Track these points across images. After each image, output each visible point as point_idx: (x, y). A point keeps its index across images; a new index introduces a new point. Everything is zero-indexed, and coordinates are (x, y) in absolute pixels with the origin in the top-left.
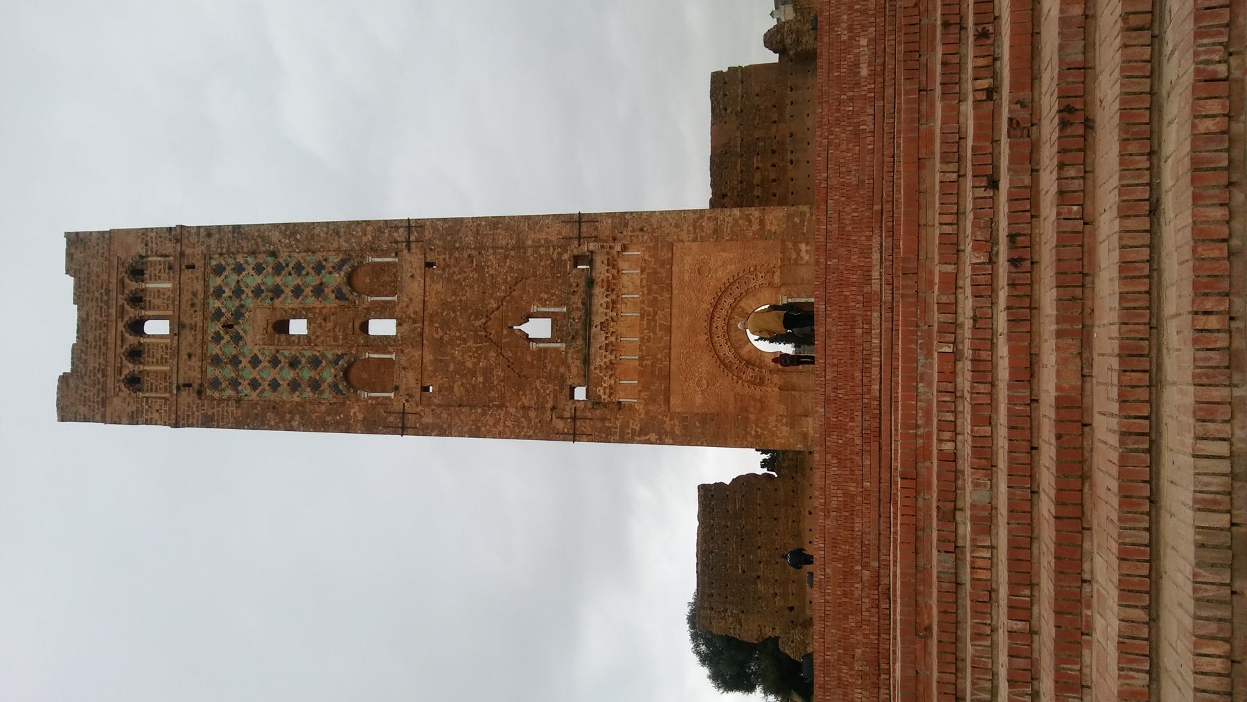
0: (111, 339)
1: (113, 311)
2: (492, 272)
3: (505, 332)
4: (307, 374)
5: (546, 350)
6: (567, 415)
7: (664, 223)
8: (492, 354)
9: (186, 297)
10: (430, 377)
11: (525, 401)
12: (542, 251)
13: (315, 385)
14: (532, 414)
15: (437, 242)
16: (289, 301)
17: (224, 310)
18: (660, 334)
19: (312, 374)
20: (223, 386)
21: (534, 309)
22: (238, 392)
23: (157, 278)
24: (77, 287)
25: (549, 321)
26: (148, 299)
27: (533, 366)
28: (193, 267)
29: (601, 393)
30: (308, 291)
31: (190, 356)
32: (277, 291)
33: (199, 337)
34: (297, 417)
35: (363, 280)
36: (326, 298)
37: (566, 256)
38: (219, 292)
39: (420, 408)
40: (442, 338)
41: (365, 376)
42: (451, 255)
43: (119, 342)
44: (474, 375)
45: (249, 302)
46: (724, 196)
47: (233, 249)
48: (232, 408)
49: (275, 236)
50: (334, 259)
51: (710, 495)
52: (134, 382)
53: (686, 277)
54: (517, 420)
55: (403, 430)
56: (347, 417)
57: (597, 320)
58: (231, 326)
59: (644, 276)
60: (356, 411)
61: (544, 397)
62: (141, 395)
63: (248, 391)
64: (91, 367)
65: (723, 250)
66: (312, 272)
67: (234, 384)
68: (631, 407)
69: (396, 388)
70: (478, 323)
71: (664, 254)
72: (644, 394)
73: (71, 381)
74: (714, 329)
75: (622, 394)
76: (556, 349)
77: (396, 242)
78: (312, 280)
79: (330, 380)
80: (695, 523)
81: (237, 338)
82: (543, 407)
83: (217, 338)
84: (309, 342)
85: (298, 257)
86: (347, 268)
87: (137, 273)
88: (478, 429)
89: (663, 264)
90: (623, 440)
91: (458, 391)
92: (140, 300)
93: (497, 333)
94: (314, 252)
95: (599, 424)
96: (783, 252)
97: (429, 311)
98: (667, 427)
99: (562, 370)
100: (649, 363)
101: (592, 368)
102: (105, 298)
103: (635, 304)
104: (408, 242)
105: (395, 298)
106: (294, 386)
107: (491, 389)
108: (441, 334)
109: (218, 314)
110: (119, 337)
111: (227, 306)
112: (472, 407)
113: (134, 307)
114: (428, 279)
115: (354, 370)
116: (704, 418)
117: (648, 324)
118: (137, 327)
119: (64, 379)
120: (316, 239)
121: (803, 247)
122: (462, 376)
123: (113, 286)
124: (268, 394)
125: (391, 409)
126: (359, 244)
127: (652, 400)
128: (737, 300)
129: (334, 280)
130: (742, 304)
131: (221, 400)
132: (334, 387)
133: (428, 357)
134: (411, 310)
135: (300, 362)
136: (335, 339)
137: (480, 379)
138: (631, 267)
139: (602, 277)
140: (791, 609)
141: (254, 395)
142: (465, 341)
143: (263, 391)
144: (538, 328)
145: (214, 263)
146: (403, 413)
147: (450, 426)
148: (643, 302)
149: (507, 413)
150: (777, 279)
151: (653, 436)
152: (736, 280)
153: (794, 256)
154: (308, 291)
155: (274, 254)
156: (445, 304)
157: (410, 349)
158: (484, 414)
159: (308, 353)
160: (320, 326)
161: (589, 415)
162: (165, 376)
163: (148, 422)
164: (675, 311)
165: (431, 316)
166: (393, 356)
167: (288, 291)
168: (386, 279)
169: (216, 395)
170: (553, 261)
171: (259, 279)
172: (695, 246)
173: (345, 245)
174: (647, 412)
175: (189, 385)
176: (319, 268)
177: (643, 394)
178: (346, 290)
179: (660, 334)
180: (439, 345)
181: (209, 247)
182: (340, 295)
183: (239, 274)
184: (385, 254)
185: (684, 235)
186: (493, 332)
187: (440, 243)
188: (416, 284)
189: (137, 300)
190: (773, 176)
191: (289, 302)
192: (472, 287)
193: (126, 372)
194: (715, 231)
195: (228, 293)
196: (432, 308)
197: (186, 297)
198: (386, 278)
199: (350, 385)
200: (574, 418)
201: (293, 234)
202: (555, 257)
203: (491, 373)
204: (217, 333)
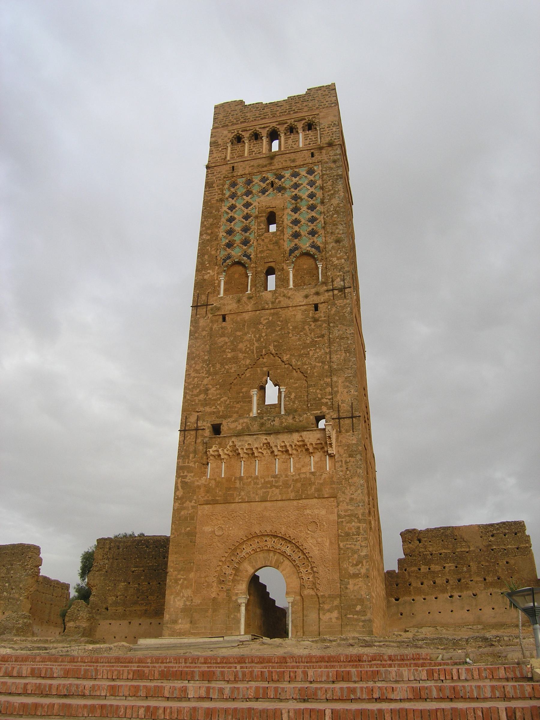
2: (311, 353)
3: (265, 369)
4: (237, 238)
5: (250, 402)
6: (200, 424)
7: (353, 488)
8: (248, 362)
10: (232, 320)
11: (212, 391)
12: (329, 389)
13: (230, 245)
14: (202, 397)
15: (334, 309)
16: (289, 218)
17: (283, 180)
18: (261, 492)
21: (283, 389)
24: (299, 97)
25: (276, 402)
28: (313, 155)
29: (214, 448)
30: (296, 228)
32: (296, 210)
34: (209, 237)
35: (306, 263)
36: (291, 241)
37: (324, 409)
39: (210, 316)
40: (261, 323)
41: (236, 276)
42: (324, 321)
43: (263, 126)
44: (233, 350)
45: (288, 195)
46: (420, 541)
47: (325, 177)
48: (217, 197)
52: (239, 139)
53: (308, 512)
55: (196, 306)
56: (207, 268)
57: (271, 439)
58: (272, 186)
59: (308, 475)
61: (214, 405)
62: (229, 145)
65: (331, 543)
66: (310, 228)
67: (233, 196)
68: (204, 473)
70: (271, 348)
71: (327, 491)
73: (240, 107)
74: (265, 539)
75: (214, 465)
76: (251, 410)
77: (332, 281)
79: (233, 253)
81: (264, 191)
82: (207, 405)
84: (259, 236)
85: (321, 218)
87: (310, 126)
88: (193, 359)
89: (318, 490)
90: (179, 468)
91: (221, 341)
92: (291, 132)
93: (264, 363)
95: (192, 449)
96: (330, 597)
97: (281, 312)
98: (188, 504)
99: (235, 415)
100: (238, 485)
101: (233, 439)
104: (333, 290)
107: (222, 364)
109: (280, 177)
110: (265, 125)
112: (209, 352)
113: (286, 129)
114: (305, 307)
115: (241, 268)
116: (192, 534)
117: (268, 482)
119: (242, 102)
121: (335, 614)
122: (232, 342)
124: (226, 217)
125: (210, 295)
128: (288, 557)
129: (305, 244)
130: (287, 562)
132: (229, 257)
133: (246, 316)
134: (281, 299)
135: (246, 232)
137: (229, 356)
138: (316, 463)
139: (306, 440)
140: (107, 609)
141: (225, 209)
142: (258, 340)
143: (227, 213)
144: (272, 394)
145: (315, 168)
146: (207, 305)
147: (196, 338)
148: (287, 476)
149: (204, 378)
150: (306, 592)
151: (180, 493)
152: (306, 557)
153: (326, 607)
154: (296, 228)
155: (322, 202)
156: (286, 322)
158: (204, 361)
159: (252, 237)
161: (199, 441)
163: (211, 152)
164: (280, 504)
165: (277, 314)
166: (249, 292)
167: (296, 216)
169: (226, 186)
170: (320, 399)
172: (334, 517)
173: (330, 247)
174: (199, 487)
177: (213, 482)
180: (255, 323)
181: (327, 163)
183: (308, 184)
184: (325, 275)
185: (343, 506)
186: (265, 360)
188: (301, 299)
189: (292, 130)
190: (438, 581)
192: (299, 340)
193: (243, 133)
194: (348, 534)
195: (295, 180)
196: (282, 312)
197: (292, 156)
198: (307, 278)
199: (229, 267)
202: (324, 401)
203: (234, 363)
204: (267, 179)
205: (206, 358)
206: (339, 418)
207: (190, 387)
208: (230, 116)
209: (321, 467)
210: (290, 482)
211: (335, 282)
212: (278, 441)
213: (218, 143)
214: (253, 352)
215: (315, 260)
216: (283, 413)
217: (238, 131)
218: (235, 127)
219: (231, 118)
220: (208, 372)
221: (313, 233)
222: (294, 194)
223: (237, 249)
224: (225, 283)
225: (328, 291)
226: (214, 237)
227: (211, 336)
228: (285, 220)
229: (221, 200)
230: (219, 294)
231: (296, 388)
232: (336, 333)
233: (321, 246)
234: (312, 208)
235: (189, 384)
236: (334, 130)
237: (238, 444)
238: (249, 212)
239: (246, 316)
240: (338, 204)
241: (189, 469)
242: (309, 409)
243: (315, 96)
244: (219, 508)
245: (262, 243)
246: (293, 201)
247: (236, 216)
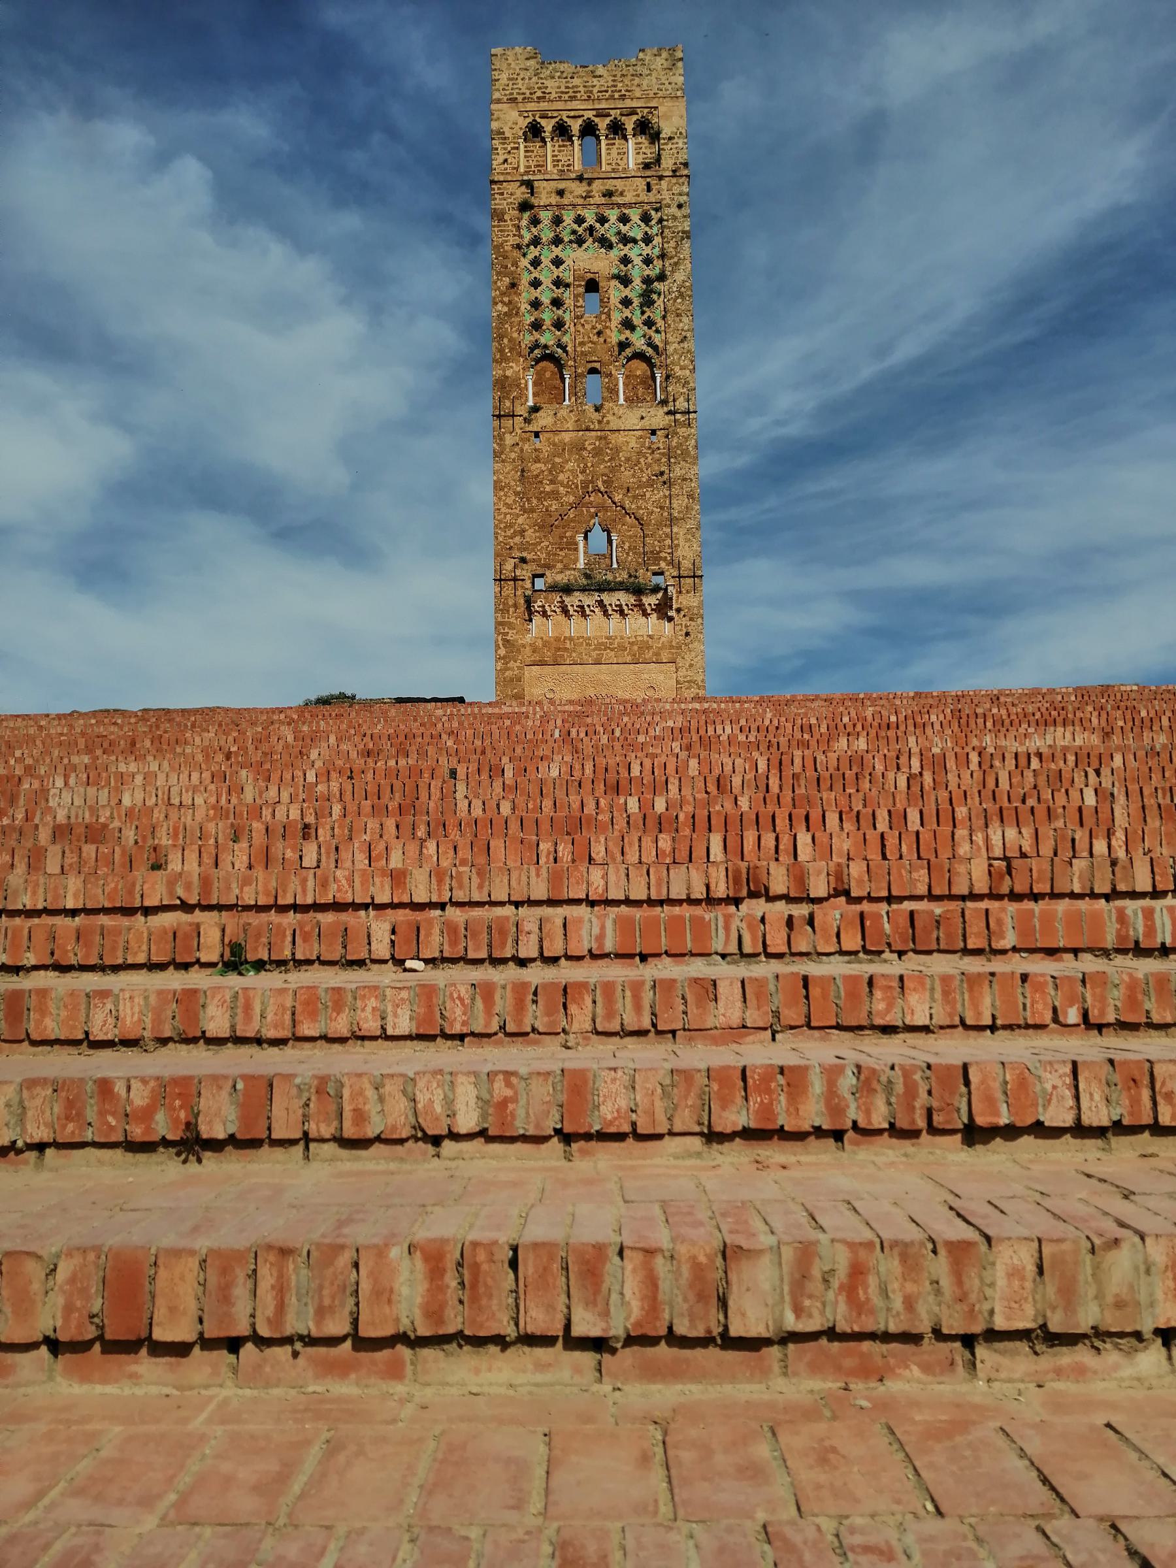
1: (603, 105)
3: (592, 510)
4: (547, 316)
5: (576, 549)
7: (693, 654)
8: (572, 499)
9: (619, 185)
11: (530, 532)
12: (668, 542)
13: (537, 326)
14: (517, 539)
16: (617, 294)
17: (606, 225)
18: (594, 654)
19: (548, 322)
20: (533, 230)
22: (528, 246)
26: (617, 142)
27: (561, 538)
28: (649, 189)
30: (627, 313)
31: (561, 193)
33: (580, 201)
34: (506, 309)
35: (640, 368)
37: (663, 564)
38: (624, 219)
39: (519, 431)
41: (548, 374)
42: (663, 454)
43: (572, 113)
44: (552, 482)
45: (615, 254)
47: (667, 231)
48: (513, 240)
50: (658, 339)
52: (534, 131)
54: (511, 526)
56: (507, 360)
57: (606, 598)
63: (530, 257)
64: (548, 83)
66: (645, 316)
67: (536, 241)
69: (535, 409)
70: (600, 484)
72: (539, 643)
76: (576, 560)
77: (674, 401)
78: (637, 320)
79: (543, 341)
81: (580, 242)
82: (525, 550)
83: (580, 220)
84: (577, 317)
86: (650, 352)
88: (502, 489)
90: (499, 624)
91: (536, 468)
93: (591, 503)
94: (664, 317)
95: (511, 602)
98: (511, 664)
99: (559, 566)
102: (617, 95)
103: (621, 631)
105: (621, 401)
106: (536, 304)
107: (539, 499)
108: (589, 448)
109: (602, 220)
113: (609, 127)
114: (640, 433)
120: (677, 319)
122: (550, 471)
123: (629, 103)
124: (526, 279)
125: (517, 402)
126: (672, 363)
129: (639, 343)
131: (518, 228)
132: (536, 345)
133: (567, 437)
136: (582, 344)
137: (548, 489)
141: (525, 262)
146: (513, 416)
149: (518, 516)
151: (502, 652)
154: (627, 313)
155: (662, 277)
156: (617, 450)
157: (574, 419)
158: (517, 494)
159: (567, 317)
160: (593, 328)
161: (519, 593)
162: (541, 166)
165: (605, 438)
166: (567, 402)
167: (627, 292)
169: (524, 223)
170: (658, 553)
171: (637, 261)
173: (671, 349)
174: (524, 646)
175: (532, 194)
176: (649, 323)
177: (540, 641)
178: (628, 352)
179: (594, 654)
180: (579, 447)
181: (669, 206)
182: (623, 346)
184: (664, 389)
187: (674, 444)
188: (636, 421)
189: (616, 129)
192: (633, 476)
196: (613, 437)
197: (619, 185)
198: (641, 390)
199: (538, 361)
200: (515, 579)
202: (663, 555)
205: (519, 489)
206: (679, 577)
207: (502, 526)
208: (519, 81)
210: (627, 645)
211: (677, 403)
213: (503, 133)
214: (577, 487)
216: (615, 566)
217: (534, 116)
218: (531, 106)
219: (520, 86)
220: (524, 510)
222: (622, 253)
223: (547, 335)
224: (535, 384)
225: (669, 413)
228: (612, 297)
230: (527, 400)
231: (630, 537)
232: (678, 472)
233: (661, 345)
234: (647, 281)
235: (500, 521)
236: (680, 145)
237: (567, 600)
238: (561, 275)
239: (567, 437)
240: (684, 281)
241: (511, 626)
243: (652, 67)
244: (547, 669)
245: (582, 330)
246: (622, 266)
247: (542, 278)
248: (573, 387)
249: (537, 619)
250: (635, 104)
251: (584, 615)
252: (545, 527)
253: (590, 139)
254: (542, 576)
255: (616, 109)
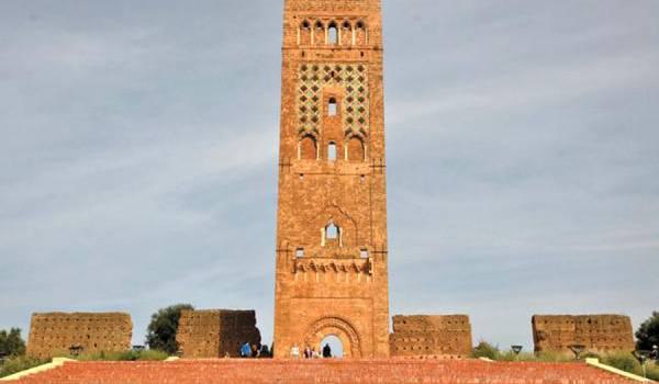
0: (326, 13)
4: (309, 115)
11: (296, 226)
13: (303, 120)
18: (329, 292)
21: (341, 229)
23: (357, 36)
28: (362, 54)
30: (350, 115)
31: (318, 55)
32: (350, 100)
35: (356, 142)
37: (367, 246)
38: (350, 69)
44: (309, 200)
49: (377, 98)
50: (366, 128)
51: (249, 317)
52: (306, 24)
56: (286, 136)
60: (291, 141)
62: (299, 30)
67: (304, 78)
68: (293, 279)
80: (235, 309)
81: (327, 79)
83: (327, 69)
86: (361, 135)
87: (360, 25)
90: (278, 275)
98: (284, 297)
106: (303, 109)
109: (339, 69)
111: (344, 75)
116: (287, 314)
118: (333, 25)
127: (297, 289)
129: (356, 129)
130: (343, 333)
132: (303, 130)
137: (307, 203)
141: (298, 88)
142: (326, 195)
151: (279, 290)
156: (343, 185)
162: (308, 42)
167: (350, 105)
168: (358, 155)
169: (299, 69)
172: (370, 310)
173: (372, 133)
180: (323, 183)
191: (344, 105)
195: (350, 74)
196: (341, 178)
198: (357, 154)
201: (379, 108)
209: (364, 280)
212: (338, 263)
215: (362, 142)
221: (361, 120)
226: (292, 112)
227: (293, 187)
229: (295, 80)
232: (375, 197)
239: (317, 177)
241: (284, 276)
242: (357, 245)
244: (304, 300)
248: (322, 151)
249: (299, 273)
250: (354, 14)
251: (324, 271)
252: (305, 223)
253: (333, 29)
254: (302, 249)
255: (346, 14)
